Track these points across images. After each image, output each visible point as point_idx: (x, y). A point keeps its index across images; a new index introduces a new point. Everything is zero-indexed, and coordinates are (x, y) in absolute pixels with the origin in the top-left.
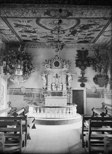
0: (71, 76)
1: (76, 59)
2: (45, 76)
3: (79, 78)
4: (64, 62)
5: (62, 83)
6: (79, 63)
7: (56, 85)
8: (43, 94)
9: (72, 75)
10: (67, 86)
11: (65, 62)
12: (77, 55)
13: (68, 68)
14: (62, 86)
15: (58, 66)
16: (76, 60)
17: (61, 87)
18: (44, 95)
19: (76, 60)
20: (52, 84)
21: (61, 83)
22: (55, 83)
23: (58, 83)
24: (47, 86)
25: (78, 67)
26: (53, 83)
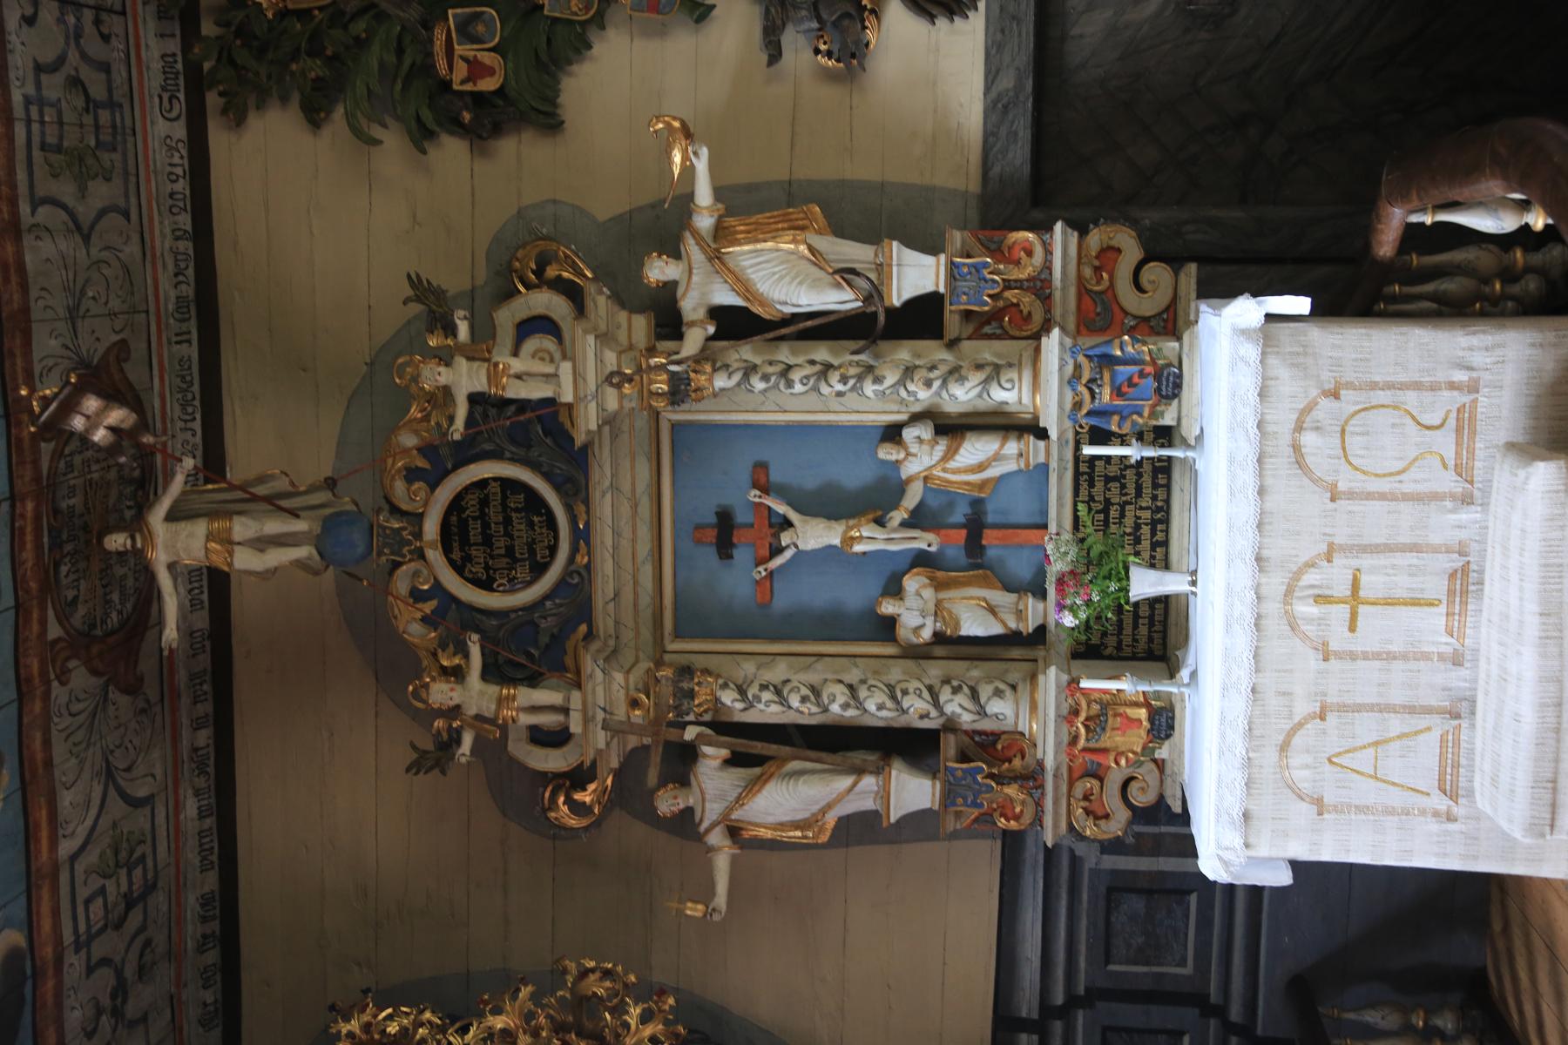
0: (744, 255)
1: (392, 140)
2: (739, 775)
3: (797, 45)
4: (447, 391)
5: (892, 434)
6: (477, 70)
7: (922, 560)
8: (1122, 815)
9: (722, 233)
10: (952, 323)
11: (444, 376)
12: (314, 115)
13: (574, 294)
14: (951, 428)
15: (534, 501)
16: (422, 136)
17: (975, 450)
18: (1141, 798)
19: (422, 136)
20: (903, 633)
21: (887, 453)
22: (894, 589)
23: (898, 516)
24: (949, 745)
25: (552, 101)
26: (887, 628)
